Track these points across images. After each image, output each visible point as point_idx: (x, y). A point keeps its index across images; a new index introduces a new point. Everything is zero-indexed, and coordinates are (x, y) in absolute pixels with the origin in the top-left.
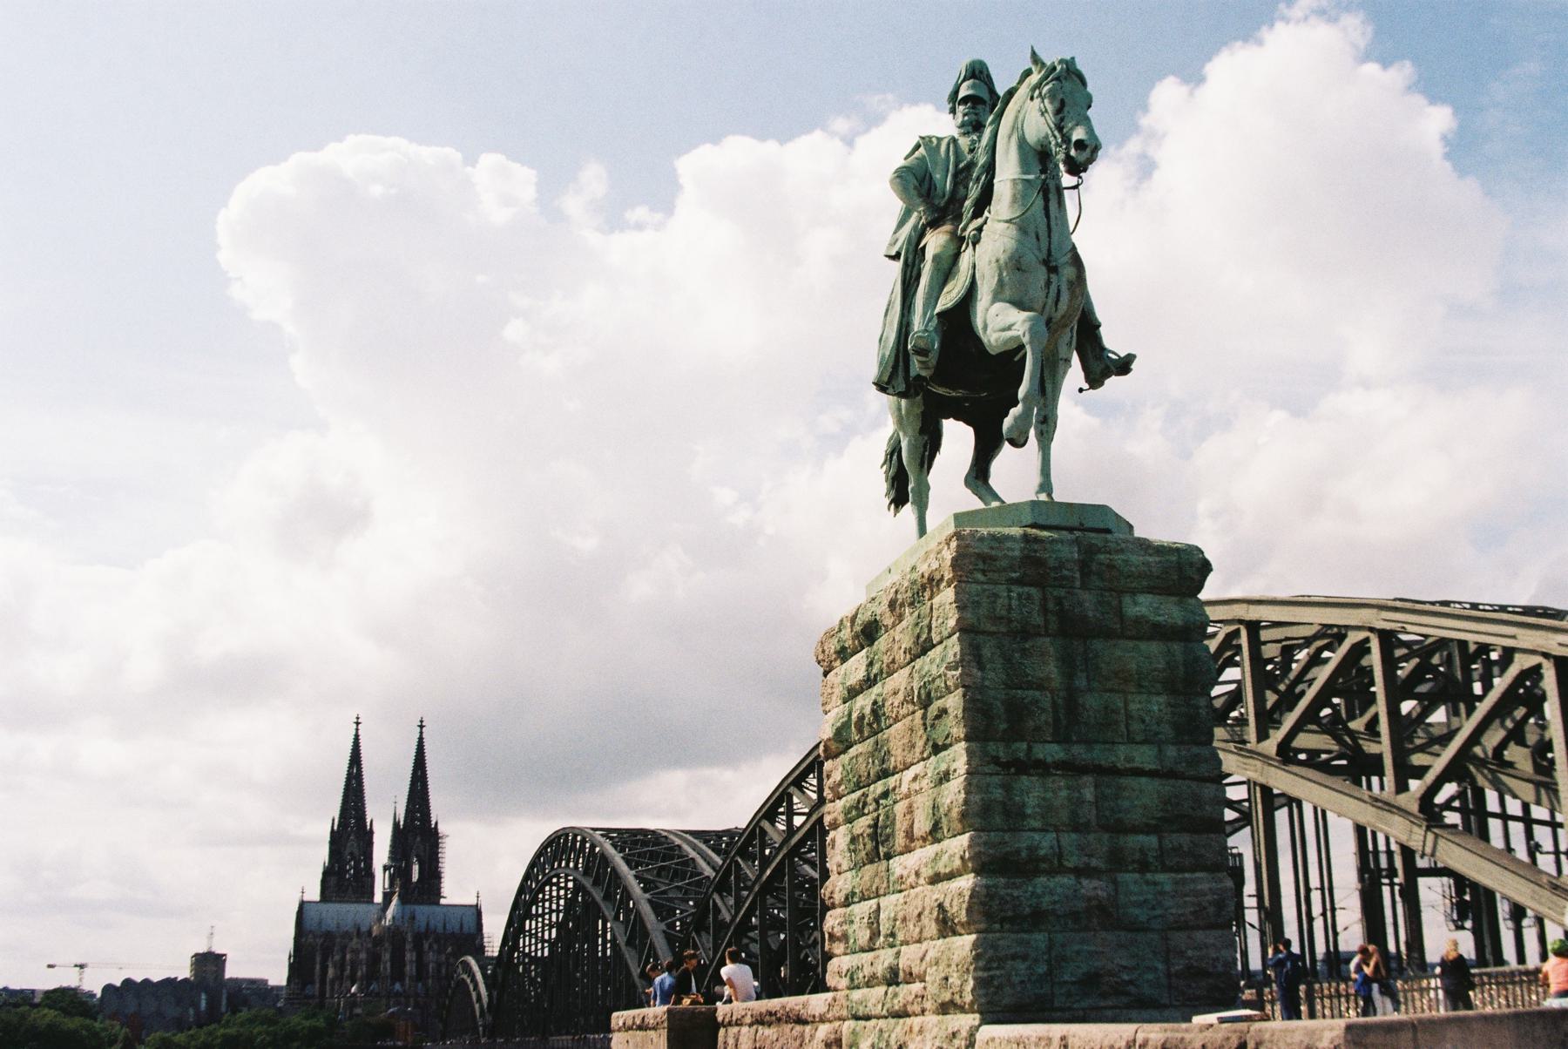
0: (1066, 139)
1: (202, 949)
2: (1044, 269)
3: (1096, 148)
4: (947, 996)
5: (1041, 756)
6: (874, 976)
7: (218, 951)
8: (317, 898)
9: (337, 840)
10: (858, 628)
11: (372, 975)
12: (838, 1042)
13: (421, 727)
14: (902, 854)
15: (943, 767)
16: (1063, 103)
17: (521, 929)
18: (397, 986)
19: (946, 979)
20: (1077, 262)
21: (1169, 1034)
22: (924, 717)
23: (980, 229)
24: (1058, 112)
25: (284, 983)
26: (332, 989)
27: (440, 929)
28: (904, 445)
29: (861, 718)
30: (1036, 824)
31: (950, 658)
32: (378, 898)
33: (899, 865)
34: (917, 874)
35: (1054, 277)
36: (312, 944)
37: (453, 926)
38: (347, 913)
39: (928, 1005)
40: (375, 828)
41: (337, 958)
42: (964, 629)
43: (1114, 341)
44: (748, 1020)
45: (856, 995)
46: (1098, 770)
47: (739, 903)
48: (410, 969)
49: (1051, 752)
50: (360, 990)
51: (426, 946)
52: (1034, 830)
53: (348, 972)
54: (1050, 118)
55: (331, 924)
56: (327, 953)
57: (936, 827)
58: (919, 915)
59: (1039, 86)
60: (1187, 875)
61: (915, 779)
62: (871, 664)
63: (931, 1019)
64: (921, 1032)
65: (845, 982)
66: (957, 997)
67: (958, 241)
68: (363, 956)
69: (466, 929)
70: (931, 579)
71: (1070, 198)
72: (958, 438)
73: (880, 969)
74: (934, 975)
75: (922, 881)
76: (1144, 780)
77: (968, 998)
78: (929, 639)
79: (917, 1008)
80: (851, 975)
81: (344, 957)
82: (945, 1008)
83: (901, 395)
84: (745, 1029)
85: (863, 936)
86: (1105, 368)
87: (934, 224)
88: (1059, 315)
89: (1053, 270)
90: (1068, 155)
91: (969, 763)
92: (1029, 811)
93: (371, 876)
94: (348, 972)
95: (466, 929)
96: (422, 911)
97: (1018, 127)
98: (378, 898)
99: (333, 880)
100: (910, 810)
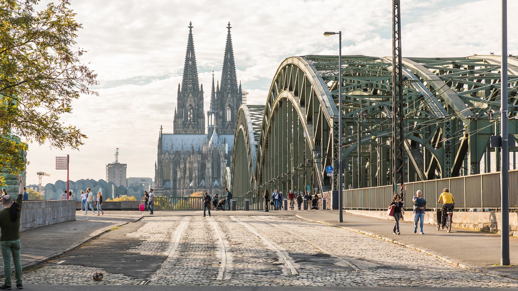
1: (112, 161)
8: (171, 131)
9: (182, 96)
11: (202, 176)
13: (229, 28)
18: (216, 182)
26: (180, 184)
32: (206, 132)
41: (182, 166)
53: (187, 174)
55: (178, 147)
56: (176, 164)
68: (196, 165)
93: (203, 117)
94: (187, 174)
98: (206, 132)
99: (180, 121)
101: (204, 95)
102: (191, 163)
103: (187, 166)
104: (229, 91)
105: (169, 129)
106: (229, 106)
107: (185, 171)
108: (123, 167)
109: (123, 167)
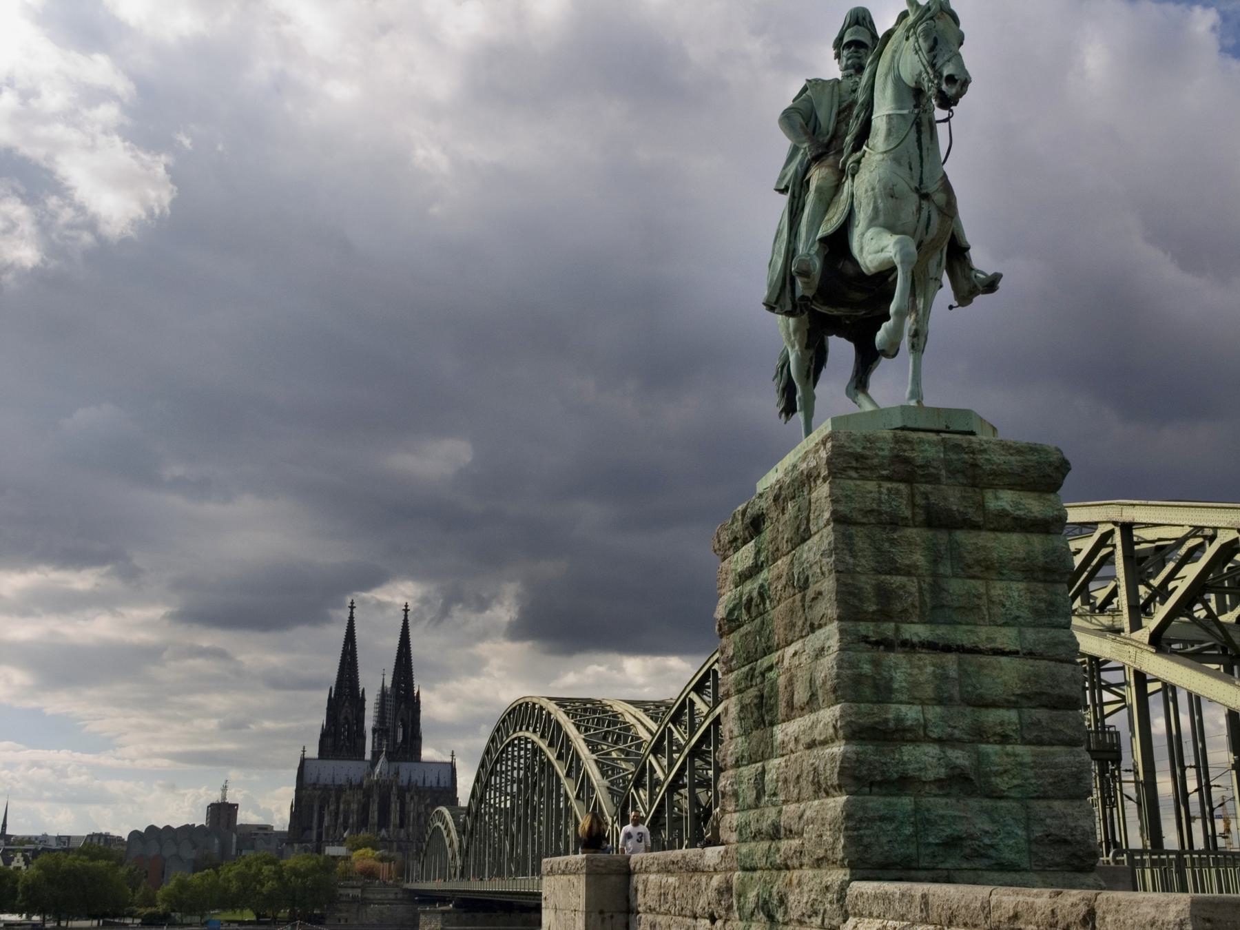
0: (938, 74)
1: (216, 797)
2: (915, 197)
3: (966, 82)
4: (820, 853)
5: (907, 636)
6: (759, 832)
7: (229, 800)
8: (316, 756)
9: (334, 706)
10: (747, 521)
12: (729, 889)
14: (784, 721)
15: (818, 645)
16: (935, 41)
17: (487, 785)
18: (383, 832)
19: (821, 836)
20: (947, 188)
21: (1021, 898)
22: (803, 598)
23: (858, 162)
24: (932, 49)
25: (287, 829)
26: (327, 835)
27: (420, 784)
28: (792, 358)
29: (750, 600)
30: (905, 697)
31: (825, 546)
32: (368, 756)
33: (782, 732)
34: (797, 740)
35: (925, 204)
36: (311, 798)
37: (431, 780)
38: (343, 770)
39: (806, 860)
40: (367, 697)
41: (332, 807)
42: (839, 519)
43: (981, 260)
44: (654, 868)
45: (744, 849)
46: (961, 649)
47: (671, 764)
48: (394, 817)
49: (917, 631)
50: (351, 833)
51: (408, 799)
52: (901, 703)
53: (341, 820)
54: (924, 57)
55: (326, 778)
56: (324, 803)
57: (813, 696)
58: (798, 777)
59: (914, 25)
60: (1046, 749)
61: (795, 654)
62: (758, 553)
63: (808, 873)
64: (799, 884)
65: (734, 837)
66: (830, 853)
67: (841, 174)
68: (354, 806)
69: (442, 784)
70: (809, 476)
71: (942, 129)
72: (841, 350)
73: (765, 825)
74: (810, 833)
75: (801, 747)
76: (1004, 659)
77: (840, 854)
78: (808, 529)
79: (796, 862)
80: (740, 829)
81: (338, 808)
82: (818, 863)
83: (789, 314)
84: (652, 877)
85: (751, 796)
86: (972, 286)
87: (817, 159)
88: (928, 238)
89: (925, 196)
90: (940, 91)
91: (841, 640)
92: (896, 686)
93: (364, 738)
94: (341, 820)
95: (442, 784)
96: (405, 768)
97: (893, 67)
98: (368, 756)
99: (329, 741)
100: (790, 682)
101: (367, 705)
102: (348, 803)
103: (342, 806)
104: (403, 700)
105: (313, 752)
106: (402, 720)
107: (337, 814)
108: (231, 809)
109: (231, 809)
